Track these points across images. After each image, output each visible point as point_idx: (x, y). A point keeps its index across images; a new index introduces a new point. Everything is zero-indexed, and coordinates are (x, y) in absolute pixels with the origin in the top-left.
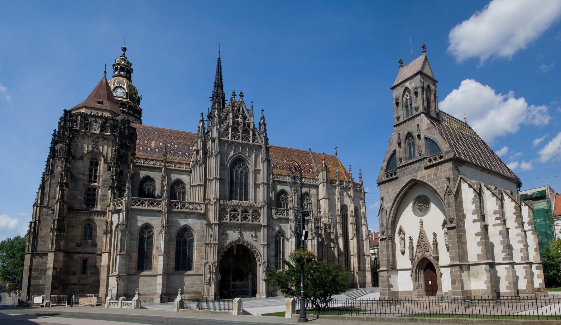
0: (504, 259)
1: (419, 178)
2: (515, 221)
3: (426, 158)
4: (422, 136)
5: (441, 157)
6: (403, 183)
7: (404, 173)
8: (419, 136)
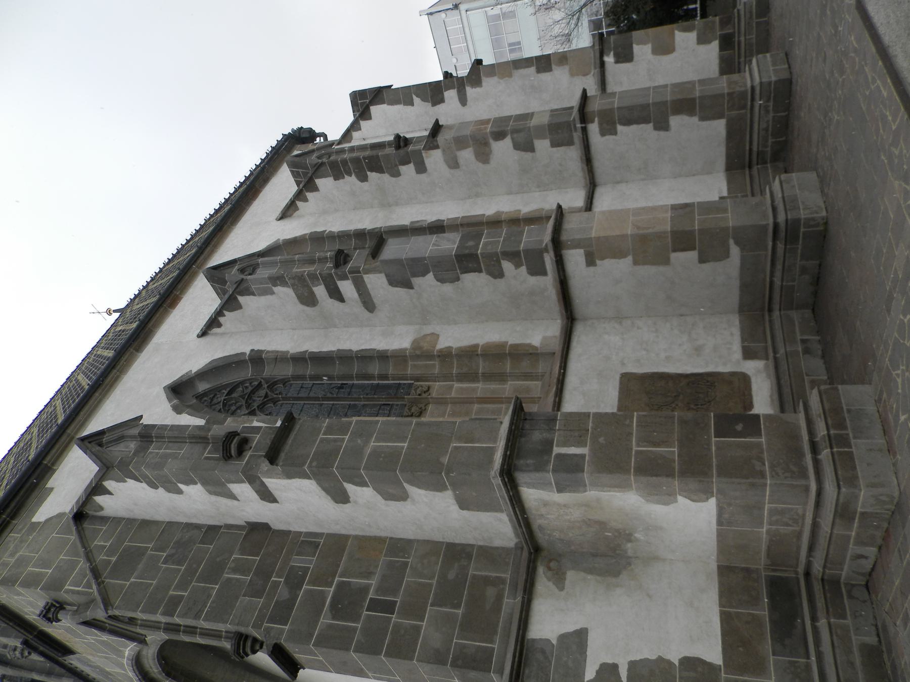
0: (537, 269)
2: (396, 174)
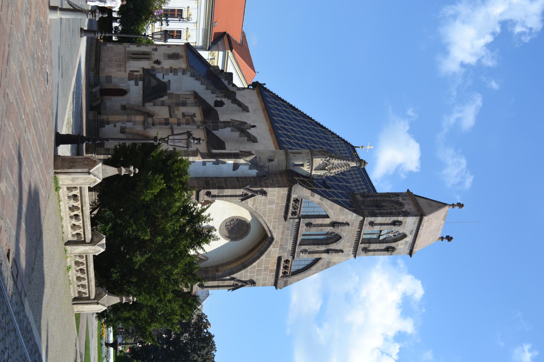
1: (271, 249)
3: (293, 258)
4: (324, 256)
5: (285, 273)
6: (274, 228)
7: (288, 229)
8: (327, 251)
